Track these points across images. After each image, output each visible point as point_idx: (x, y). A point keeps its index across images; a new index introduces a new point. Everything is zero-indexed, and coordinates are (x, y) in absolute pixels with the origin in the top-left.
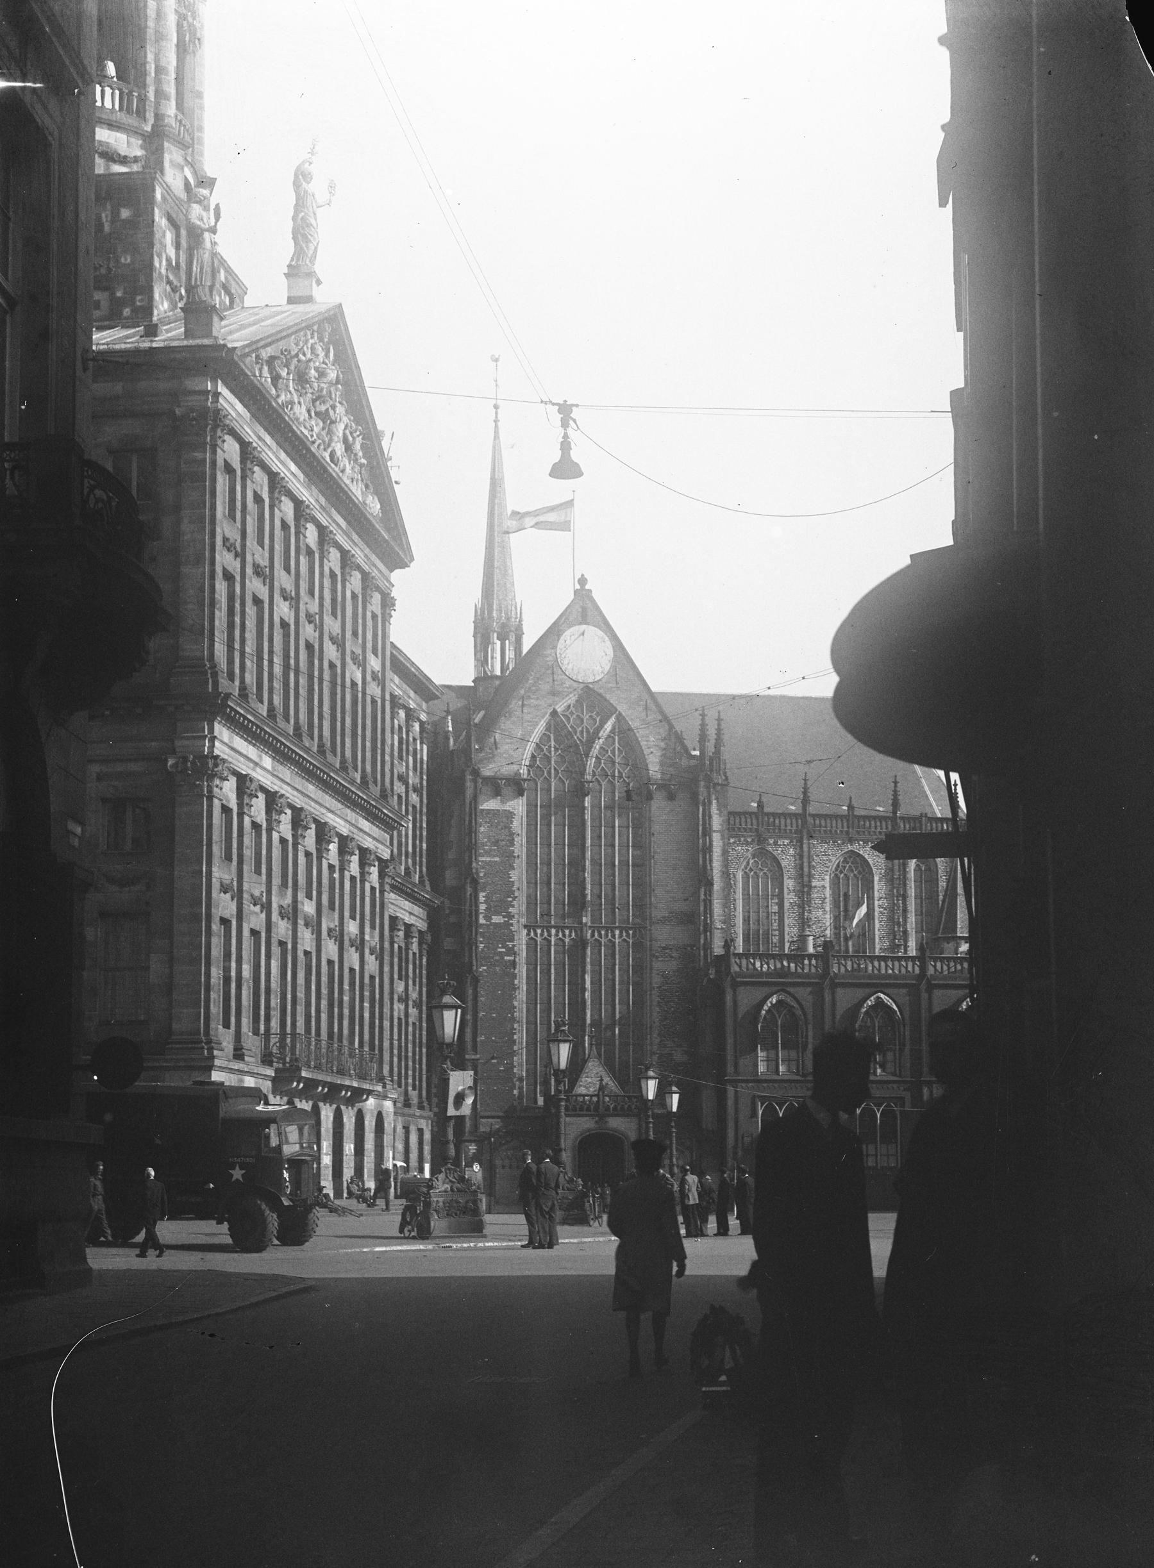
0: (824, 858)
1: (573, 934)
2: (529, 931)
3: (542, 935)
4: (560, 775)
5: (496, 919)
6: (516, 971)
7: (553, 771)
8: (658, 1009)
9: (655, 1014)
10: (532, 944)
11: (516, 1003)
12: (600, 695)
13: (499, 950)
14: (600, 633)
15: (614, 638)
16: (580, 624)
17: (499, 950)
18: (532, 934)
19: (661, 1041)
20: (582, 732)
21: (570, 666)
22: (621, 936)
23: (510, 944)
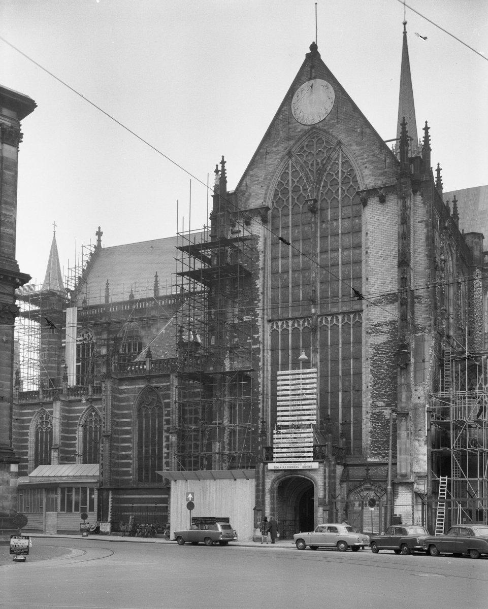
1: (306, 324)
2: (273, 324)
3: (282, 326)
4: (296, 201)
5: (247, 318)
6: (261, 356)
7: (290, 198)
10: (274, 333)
11: (260, 380)
12: (325, 131)
13: (248, 341)
14: (325, 83)
16: (310, 79)
17: (248, 341)
18: (275, 327)
21: (301, 114)
22: (343, 320)
23: (256, 336)
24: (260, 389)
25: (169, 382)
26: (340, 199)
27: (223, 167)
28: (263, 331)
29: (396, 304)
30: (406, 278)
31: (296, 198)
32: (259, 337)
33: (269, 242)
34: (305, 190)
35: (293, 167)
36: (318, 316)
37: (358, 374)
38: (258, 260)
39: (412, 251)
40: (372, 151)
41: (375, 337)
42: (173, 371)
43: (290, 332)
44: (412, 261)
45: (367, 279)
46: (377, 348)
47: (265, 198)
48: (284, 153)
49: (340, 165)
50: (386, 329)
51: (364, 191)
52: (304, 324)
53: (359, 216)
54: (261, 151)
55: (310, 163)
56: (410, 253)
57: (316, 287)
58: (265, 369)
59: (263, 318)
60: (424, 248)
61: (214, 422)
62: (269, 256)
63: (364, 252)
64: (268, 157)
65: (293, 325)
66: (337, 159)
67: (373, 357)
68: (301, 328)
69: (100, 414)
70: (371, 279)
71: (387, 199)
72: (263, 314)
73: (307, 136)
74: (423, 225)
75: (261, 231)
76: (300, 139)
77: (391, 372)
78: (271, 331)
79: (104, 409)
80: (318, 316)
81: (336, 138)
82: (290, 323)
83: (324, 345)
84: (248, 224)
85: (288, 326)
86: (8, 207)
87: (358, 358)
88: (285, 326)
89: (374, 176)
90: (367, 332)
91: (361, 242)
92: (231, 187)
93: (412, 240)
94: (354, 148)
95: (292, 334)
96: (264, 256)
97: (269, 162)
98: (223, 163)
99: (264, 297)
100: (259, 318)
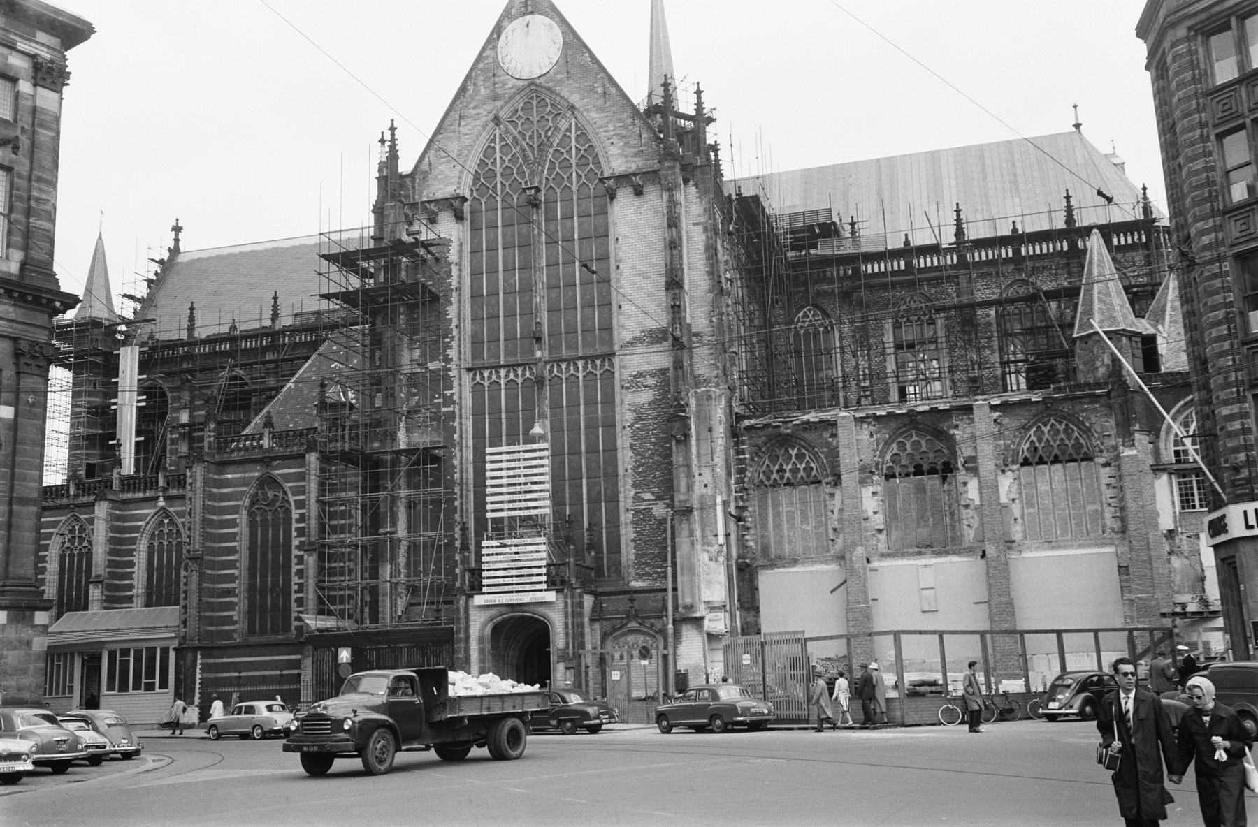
0: (987, 291)
1: (528, 374)
2: (475, 375)
3: (489, 378)
4: (507, 189)
5: (433, 366)
6: (456, 424)
7: (499, 186)
8: (630, 454)
9: (628, 459)
10: (477, 388)
11: (456, 462)
12: (548, 89)
13: (436, 401)
14: (547, 20)
15: (563, 22)
16: (524, 14)
17: (436, 401)
18: (478, 378)
19: (636, 493)
20: (531, 137)
21: (513, 64)
22: (585, 368)
23: (448, 393)
24: (457, 476)
25: (303, 466)
26: (574, 188)
27: (393, 135)
28: (460, 385)
29: (665, 344)
30: (679, 306)
31: (507, 184)
32: (453, 394)
33: (467, 248)
34: (521, 173)
35: (502, 139)
36: (546, 362)
37: (612, 449)
38: (449, 275)
39: (685, 267)
40: (620, 120)
41: (636, 394)
42: (311, 449)
43: (503, 386)
44: (686, 281)
45: (620, 307)
46: (638, 411)
47: (459, 183)
48: (488, 118)
49: (573, 139)
50: (650, 381)
51: (610, 178)
52: (523, 375)
53: (604, 212)
54: (452, 113)
55: (528, 135)
56: (682, 269)
57: (541, 317)
58: (464, 445)
59: (459, 365)
60: (703, 262)
61: (382, 531)
62: (467, 271)
63: (613, 267)
64: (463, 123)
65: (507, 376)
66: (569, 130)
67: (633, 424)
68: (520, 380)
69: (179, 521)
70: (626, 307)
71: (645, 190)
72: (459, 359)
73: (522, 94)
74: (701, 227)
75: (454, 233)
76: (511, 98)
77: (662, 447)
78: (472, 384)
79: (190, 514)
80: (546, 362)
81: (566, 100)
82: (503, 372)
83: (556, 405)
84: (433, 221)
85: (499, 377)
86: (43, 187)
87: (610, 425)
88: (494, 377)
89: (626, 156)
90: (622, 387)
91: (608, 251)
92: (406, 165)
93: (685, 250)
94: (593, 115)
95: (506, 389)
96: (460, 270)
97: (464, 130)
98: (392, 129)
99: (459, 333)
100: (453, 365)
